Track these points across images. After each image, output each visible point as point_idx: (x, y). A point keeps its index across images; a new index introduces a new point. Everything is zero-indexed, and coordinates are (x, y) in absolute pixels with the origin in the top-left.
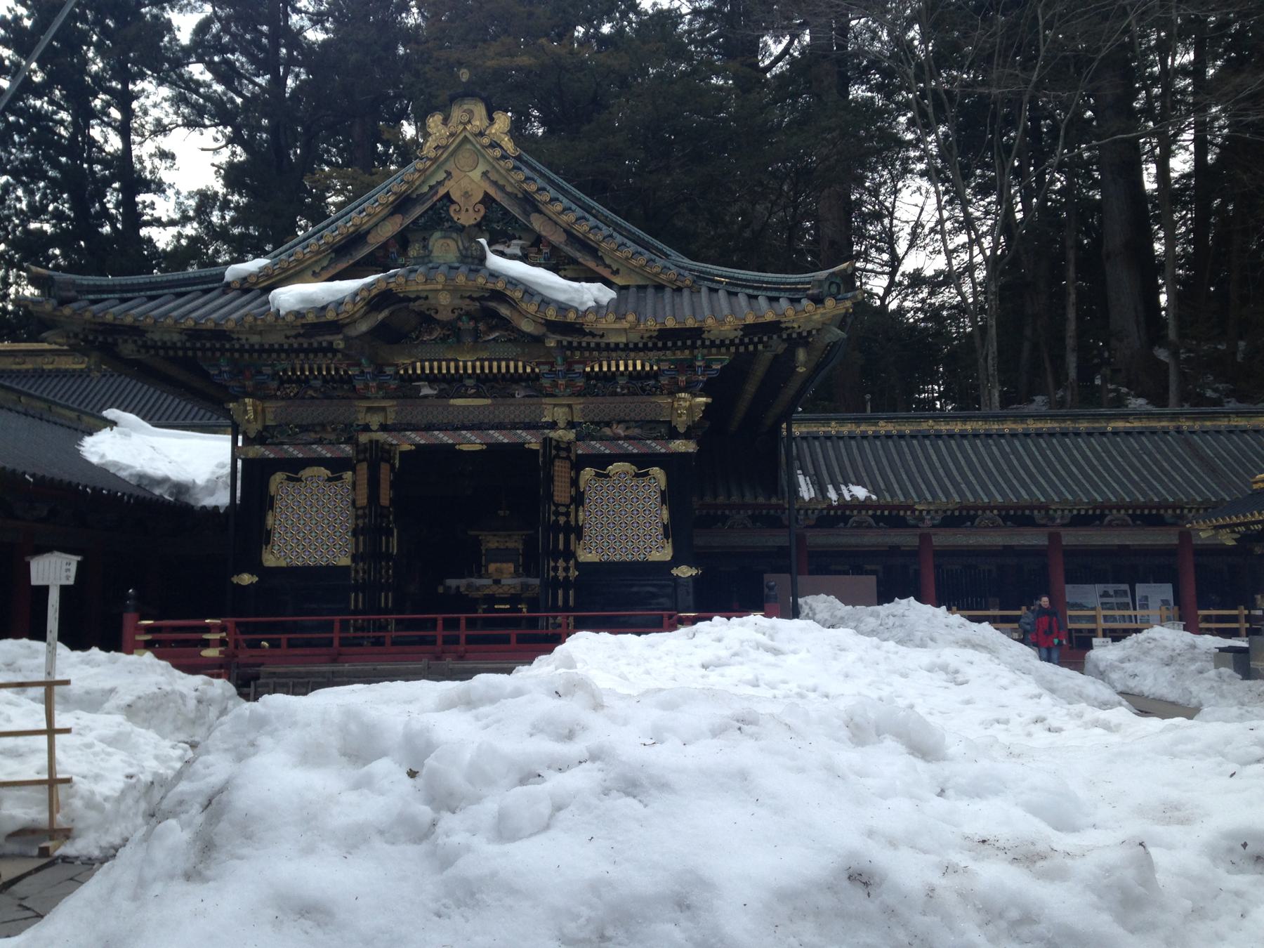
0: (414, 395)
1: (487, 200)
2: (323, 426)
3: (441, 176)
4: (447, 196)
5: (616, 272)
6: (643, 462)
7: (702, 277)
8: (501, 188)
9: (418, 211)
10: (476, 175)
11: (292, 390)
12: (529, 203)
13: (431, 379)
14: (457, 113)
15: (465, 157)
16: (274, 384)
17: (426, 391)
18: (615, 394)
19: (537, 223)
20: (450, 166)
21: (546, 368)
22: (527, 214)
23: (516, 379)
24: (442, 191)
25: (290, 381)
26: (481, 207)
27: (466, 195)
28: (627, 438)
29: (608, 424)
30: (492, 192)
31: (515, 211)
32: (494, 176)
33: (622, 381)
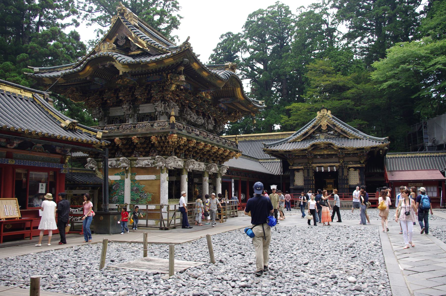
0: (316, 158)
1: (327, 125)
2: (302, 163)
3: (320, 122)
4: (321, 126)
5: (350, 136)
6: (355, 169)
7: (365, 137)
8: (330, 123)
9: (316, 128)
10: (325, 121)
11: (297, 157)
12: (334, 125)
13: (319, 155)
14: (322, 111)
15: (323, 119)
16: (294, 157)
17: (318, 157)
18: (350, 157)
19: (336, 129)
20: (321, 120)
21: (338, 153)
22: (334, 128)
23: (333, 155)
24: (320, 124)
25: (297, 156)
26: (327, 127)
27: (324, 125)
28: (352, 164)
29: (349, 162)
30: (329, 124)
31: (332, 127)
32: (328, 121)
33: (351, 154)
